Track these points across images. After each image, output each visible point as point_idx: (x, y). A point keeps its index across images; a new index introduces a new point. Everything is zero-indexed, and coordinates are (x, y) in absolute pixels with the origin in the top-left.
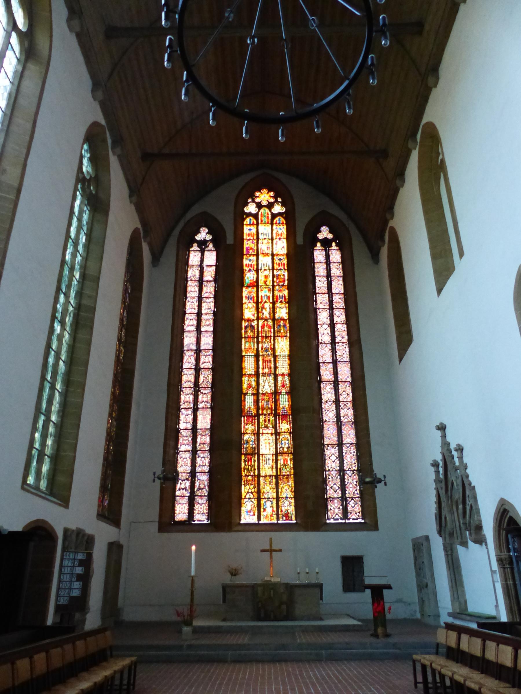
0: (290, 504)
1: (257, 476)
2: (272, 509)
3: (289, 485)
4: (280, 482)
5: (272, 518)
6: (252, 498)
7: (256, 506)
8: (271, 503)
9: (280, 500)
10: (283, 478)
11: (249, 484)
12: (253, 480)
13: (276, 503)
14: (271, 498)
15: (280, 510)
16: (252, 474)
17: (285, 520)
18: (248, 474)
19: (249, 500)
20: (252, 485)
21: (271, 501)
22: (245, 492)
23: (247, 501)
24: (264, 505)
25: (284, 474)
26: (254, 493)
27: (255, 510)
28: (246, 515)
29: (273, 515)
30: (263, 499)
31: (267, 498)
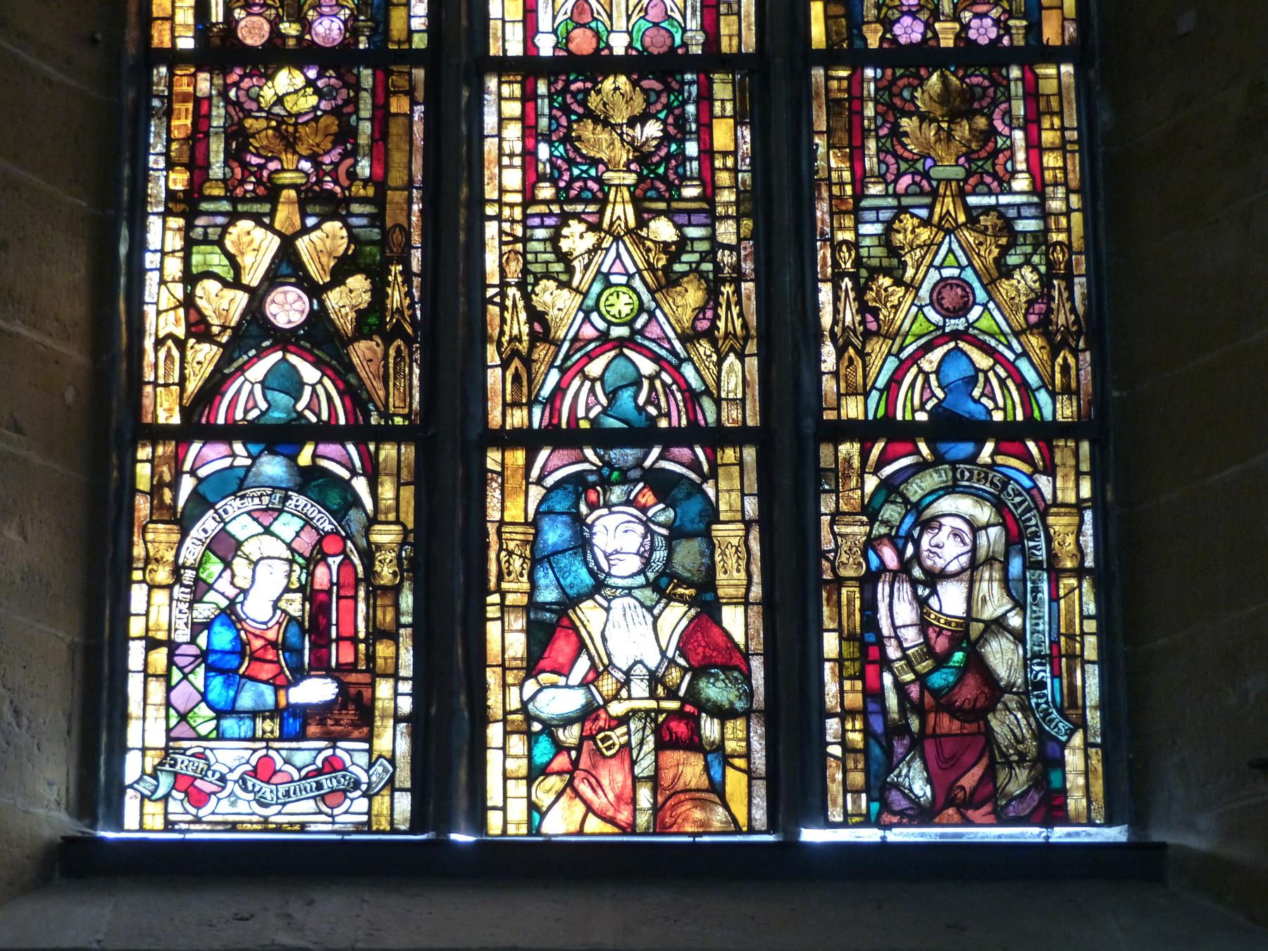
0: (1016, 537)
1: (431, 58)
2: (675, 616)
3: (1007, 226)
4: (832, 163)
5: (691, 770)
6: (326, 432)
7: (386, 573)
8: (661, 513)
9: (838, 473)
10: (892, 109)
11: (272, 193)
12: (346, 134)
13: (766, 522)
14: (671, 439)
15: (831, 644)
16: (328, 29)
17: (922, 814)
18: (253, 31)
19: (273, 468)
20: (333, 207)
21: (663, 485)
22: (199, 328)
23: (238, 483)
24: (538, 559)
25: (909, 31)
26: (363, 352)
27: (377, 634)
28: (203, 719)
29: (710, 728)
30: (529, 440)
31: (600, 437)
